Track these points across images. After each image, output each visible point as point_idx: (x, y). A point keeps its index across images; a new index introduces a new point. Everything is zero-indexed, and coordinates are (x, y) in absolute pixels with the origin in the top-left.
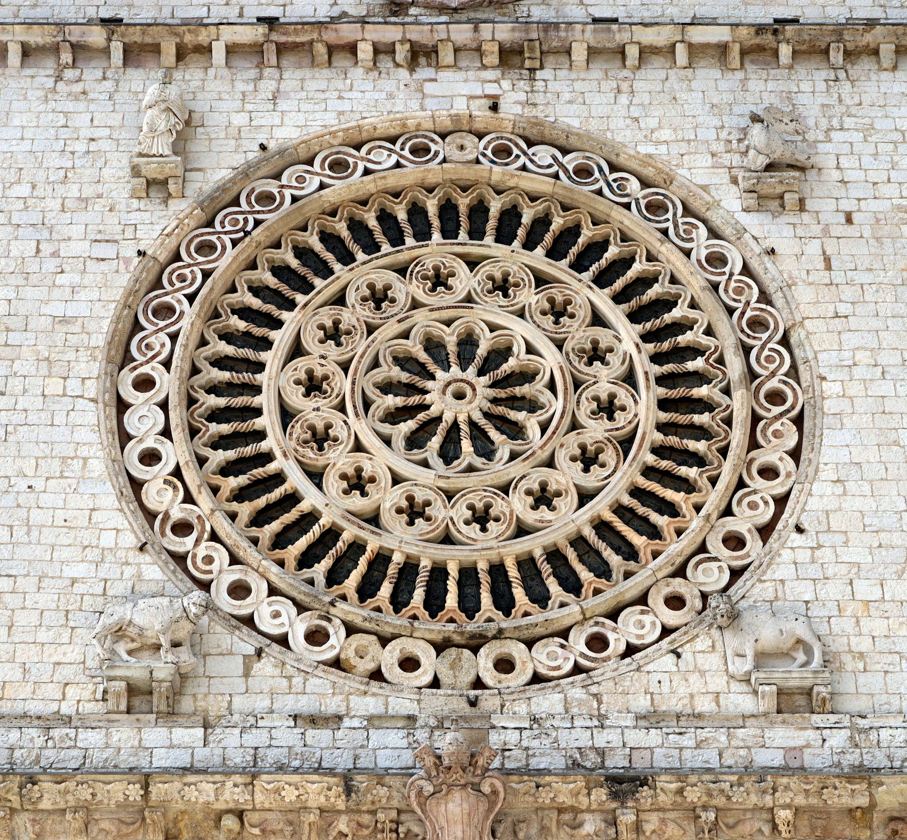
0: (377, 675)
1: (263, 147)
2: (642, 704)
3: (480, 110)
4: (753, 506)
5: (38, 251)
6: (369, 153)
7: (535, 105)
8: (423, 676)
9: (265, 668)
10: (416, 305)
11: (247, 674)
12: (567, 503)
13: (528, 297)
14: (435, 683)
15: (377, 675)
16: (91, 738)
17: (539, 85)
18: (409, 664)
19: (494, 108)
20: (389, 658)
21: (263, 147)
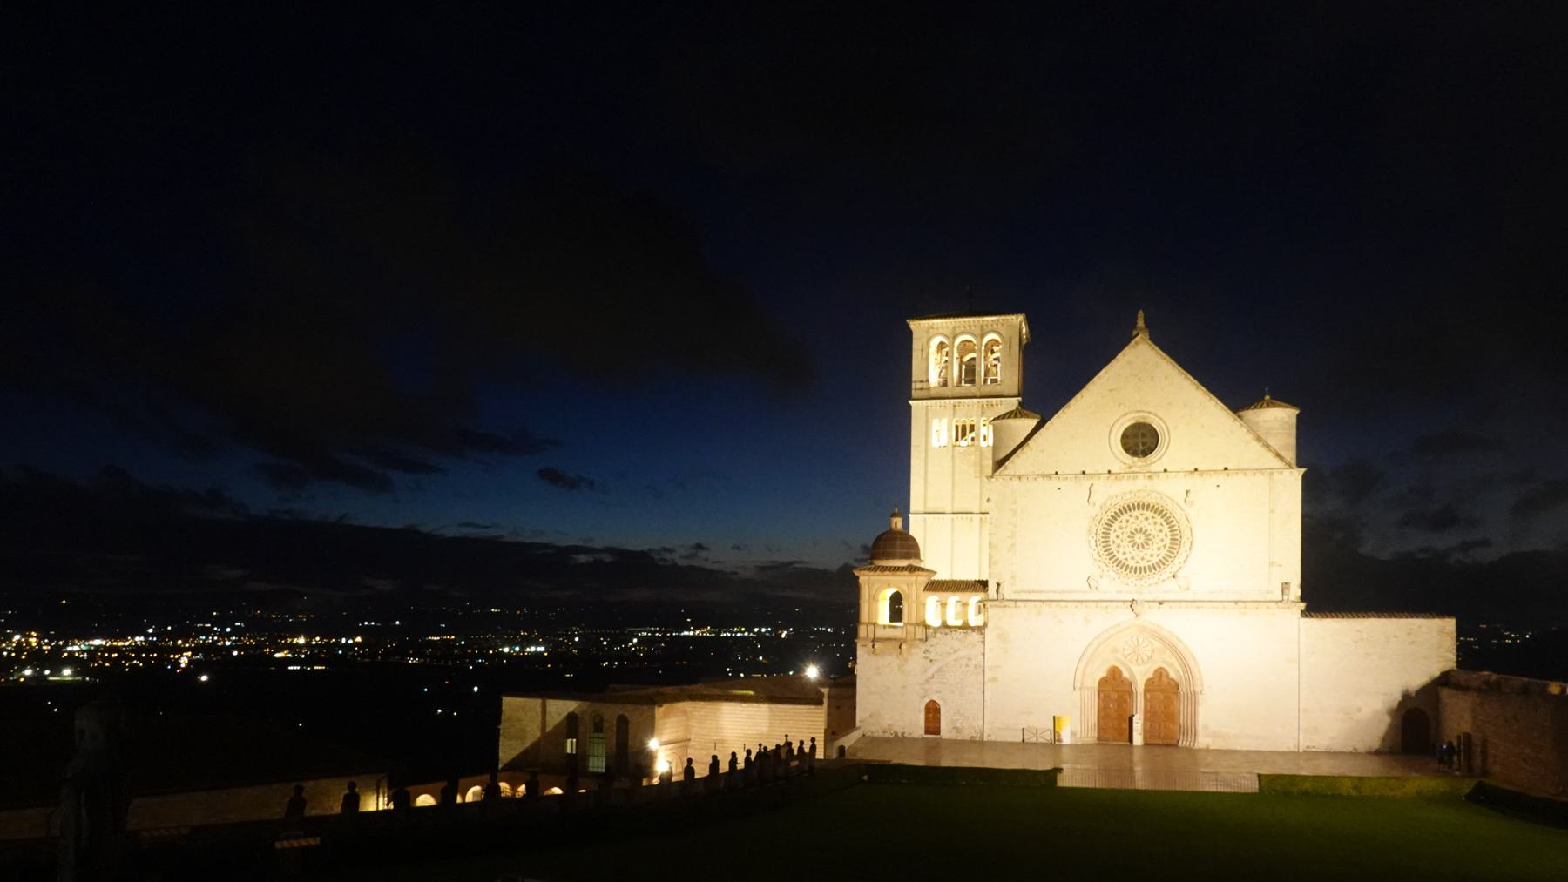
0: (1127, 584)
12: (1155, 556)
13: (1151, 521)
15: (1127, 584)
18: (1132, 582)
20: (1129, 581)
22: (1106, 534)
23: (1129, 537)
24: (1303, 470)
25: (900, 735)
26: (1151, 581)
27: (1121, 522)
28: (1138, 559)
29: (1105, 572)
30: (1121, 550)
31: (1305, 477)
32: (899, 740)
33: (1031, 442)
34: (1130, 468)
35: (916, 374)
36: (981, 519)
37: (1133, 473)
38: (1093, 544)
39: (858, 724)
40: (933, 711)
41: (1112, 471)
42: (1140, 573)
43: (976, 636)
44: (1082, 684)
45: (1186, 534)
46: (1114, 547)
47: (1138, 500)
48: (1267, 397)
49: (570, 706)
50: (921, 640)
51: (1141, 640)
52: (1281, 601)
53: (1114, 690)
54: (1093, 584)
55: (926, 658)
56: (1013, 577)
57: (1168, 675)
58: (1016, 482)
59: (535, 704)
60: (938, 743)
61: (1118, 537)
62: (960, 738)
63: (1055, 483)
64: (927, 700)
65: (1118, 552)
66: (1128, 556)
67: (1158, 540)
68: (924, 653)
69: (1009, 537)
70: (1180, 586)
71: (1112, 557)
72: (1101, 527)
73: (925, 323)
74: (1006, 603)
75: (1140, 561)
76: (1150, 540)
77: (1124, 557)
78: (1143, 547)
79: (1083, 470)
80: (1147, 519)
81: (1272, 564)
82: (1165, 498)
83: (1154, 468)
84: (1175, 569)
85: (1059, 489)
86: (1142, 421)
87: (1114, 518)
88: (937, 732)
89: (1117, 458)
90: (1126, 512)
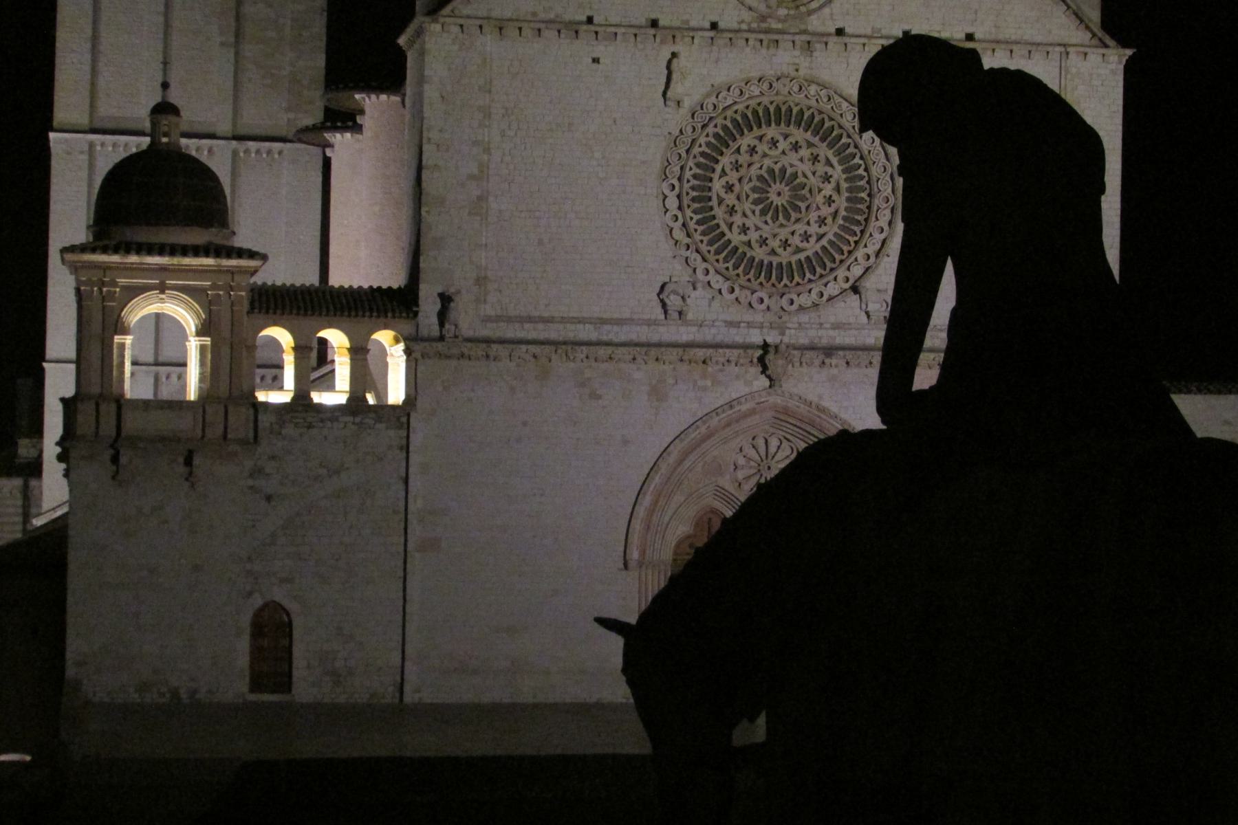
1: (713, 86)
2: (832, 319)
3: (793, 74)
4: (874, 244)
5: (633, 130)
6: (750, 87)
7: (812, 69)
8: (763, 307)
9: (716, 304)
10: (765, 155)
11: (710, 306)
13: (805, 152)
14: (768, 308)
16: (662, 329)
17: (814, 58)
19: (797, 70)
21: (713, 86)
23: (754, 190)
24: (1129, 52)
25: (184, 695)
26: (805, 300)
27: (738, 151)
28: (774, 244)
29: (700, 274)
30: (738, 219)
31: (1131, 72)
34: (763, 18)
36: (235, 153)
37: (768, 31)
38: (672, 203)
41: (722, 25)
42: (780, 279)
44: (643, 553)
46: (719, 212)
47: (779, 99)
50: (243, 442)
51: (774, 443)
54: (673, 301)
56: (481, 281)
58: (489, 42)
61: (729, 188)
62: (342, 699)
63: (584, 48)
64: (258, 601)
65: (730, 226)
66: (753, 236)
67: (819, 199)
68: (251, 476)
69: (471, 177)
71: (716, 236)
74: (466, 348)
75: (780, 251)
76: (804, 199)
77: (744, 238)
78: (787, 217)
79: (653, 16)
80: (796, 147)
82: (838, 99)
83: (814, 23)
84: (857, 271)
85: (596, 60)
87: (724, 140)
88: (284, 682)
90: (751, 129)
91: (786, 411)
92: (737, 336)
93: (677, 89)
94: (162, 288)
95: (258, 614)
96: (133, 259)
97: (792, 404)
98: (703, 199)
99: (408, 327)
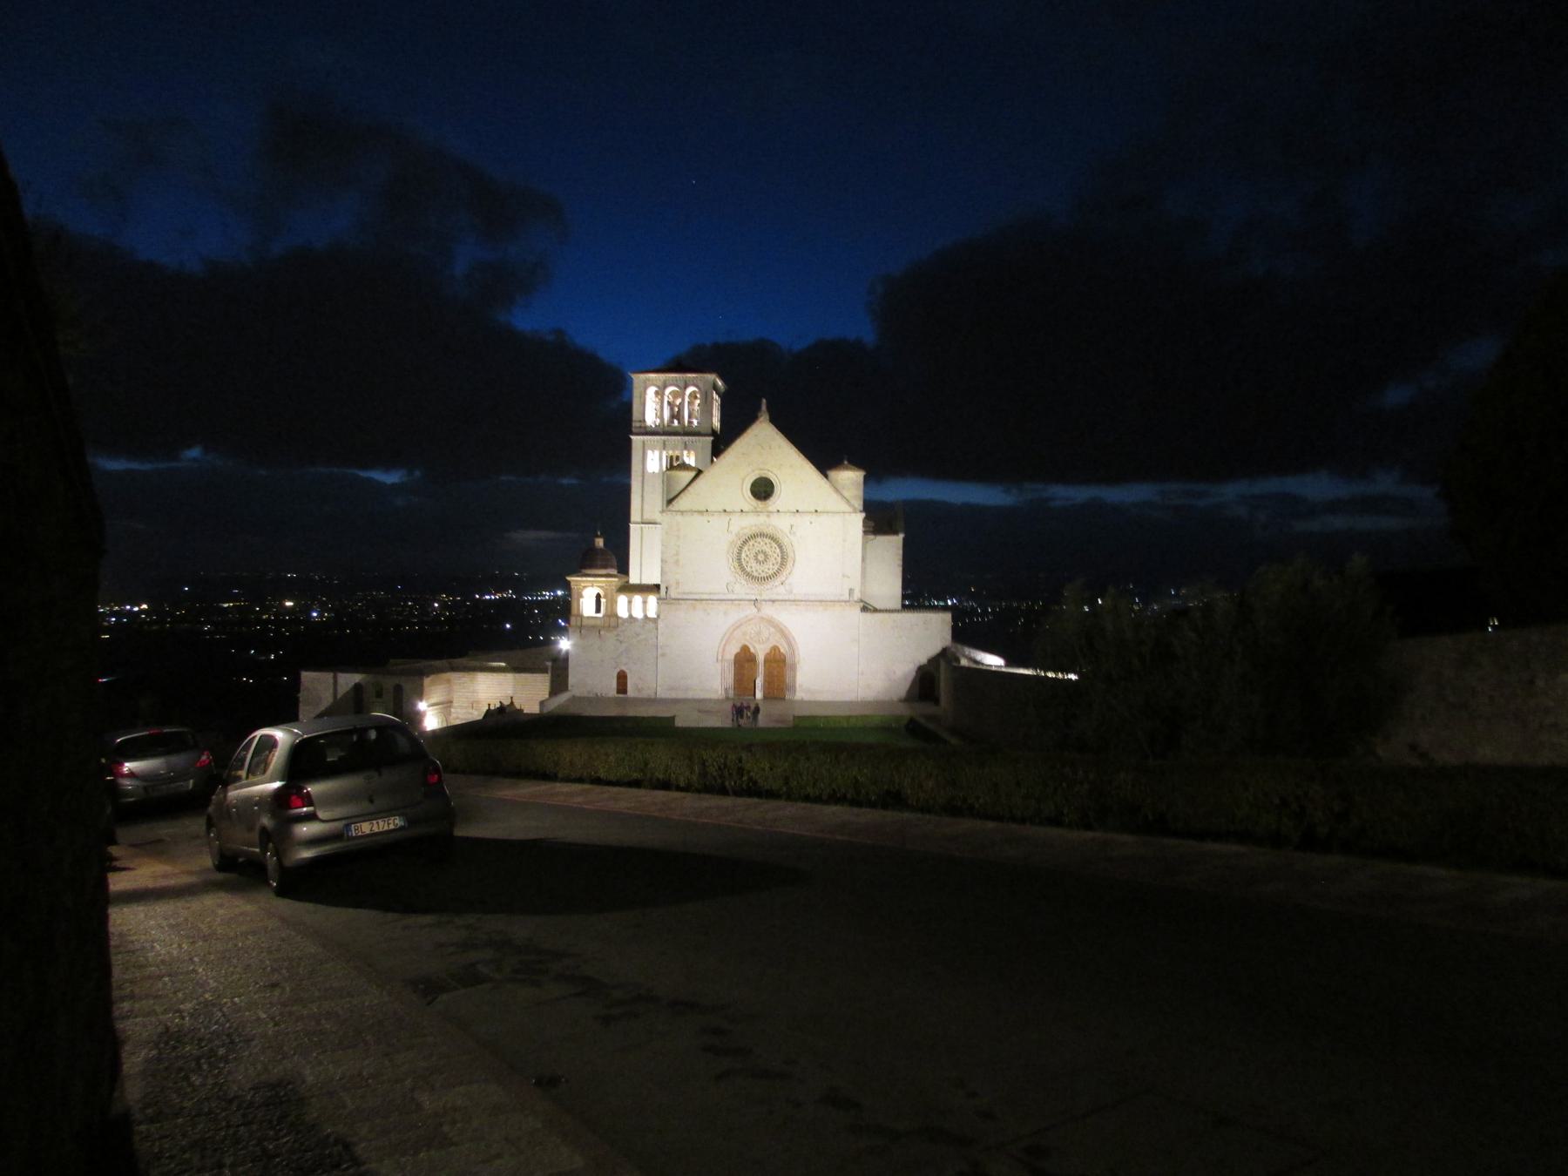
22: (739, 553)
32: (598, 700)
33: (689, 488)
35: (636, 415)
38: (731, 560)
39: (569, 688)
40: (622, 678)
43: (652, 625)
44: (722, 657)
45: (791, 554)
48: (846, 462)
49: (356, 678)
52: (848, 601)
53: (744, 660)
54: (730, 588)
55: (617, 640)
57: (779, 649)
59: (327, 677)
60: (627, 700)
61: (747, 556)
63: (705, 518)
64: (619, 670)
70: (786, 590)
71: (743, 569)
72: (736, 549)
73: (643, 376)
81: (844, 576)
83: (770, 509)
86: (764, 476)
87: (745, 542)
89: (746, 499)
91: (762, 618)
92: (748, 597)
93: (731, 528)
94: (592, 586)
95: (619, 673)
96: (584, 579)
97: (764, 616)
98: (739, 559)
99: (658, 596)
